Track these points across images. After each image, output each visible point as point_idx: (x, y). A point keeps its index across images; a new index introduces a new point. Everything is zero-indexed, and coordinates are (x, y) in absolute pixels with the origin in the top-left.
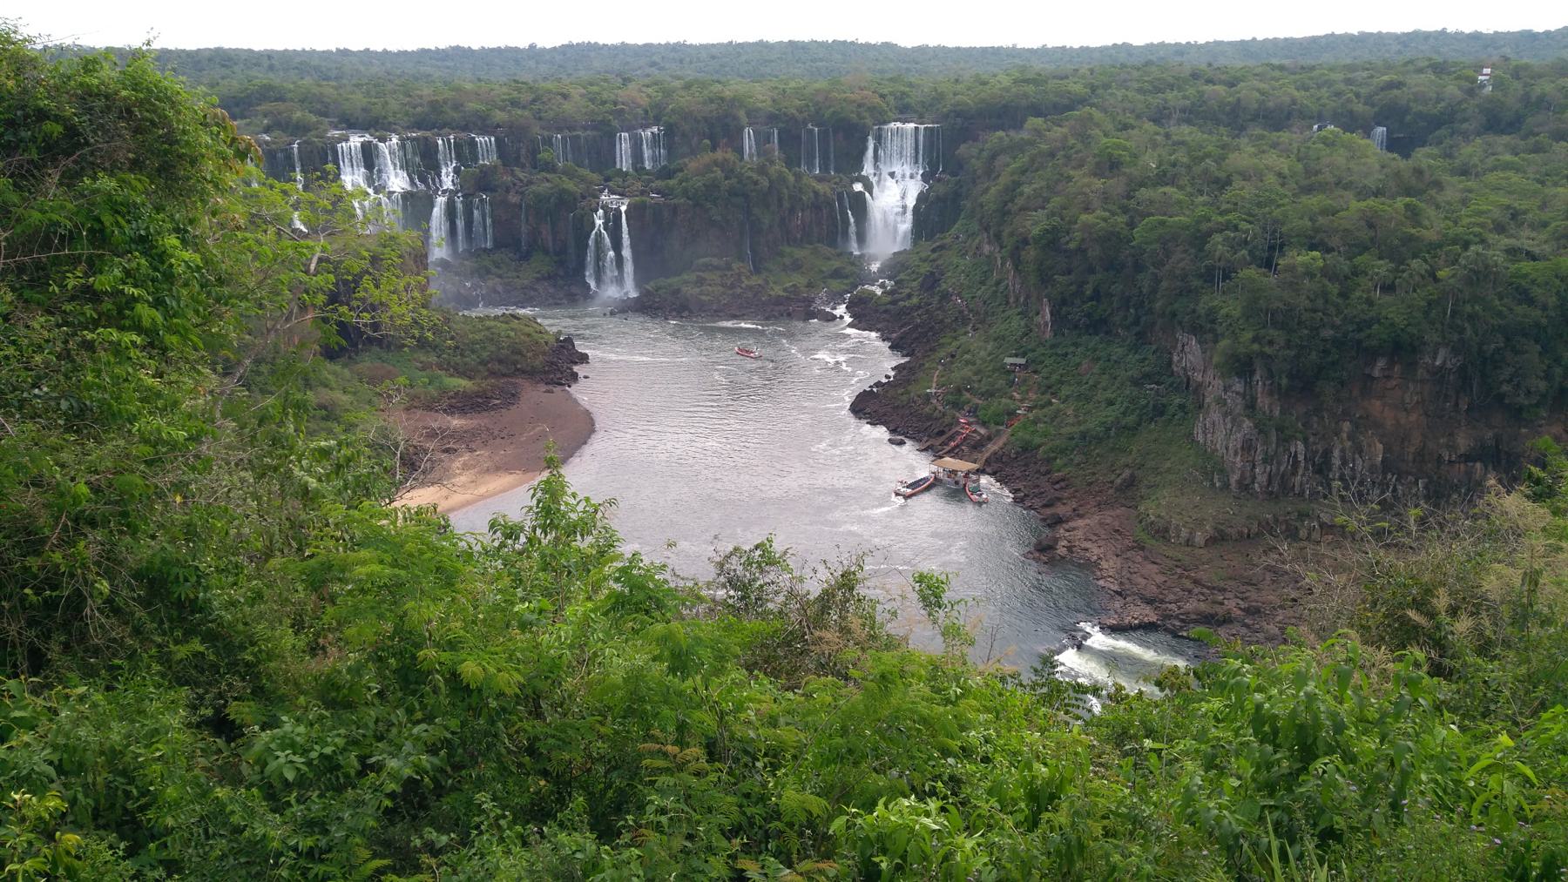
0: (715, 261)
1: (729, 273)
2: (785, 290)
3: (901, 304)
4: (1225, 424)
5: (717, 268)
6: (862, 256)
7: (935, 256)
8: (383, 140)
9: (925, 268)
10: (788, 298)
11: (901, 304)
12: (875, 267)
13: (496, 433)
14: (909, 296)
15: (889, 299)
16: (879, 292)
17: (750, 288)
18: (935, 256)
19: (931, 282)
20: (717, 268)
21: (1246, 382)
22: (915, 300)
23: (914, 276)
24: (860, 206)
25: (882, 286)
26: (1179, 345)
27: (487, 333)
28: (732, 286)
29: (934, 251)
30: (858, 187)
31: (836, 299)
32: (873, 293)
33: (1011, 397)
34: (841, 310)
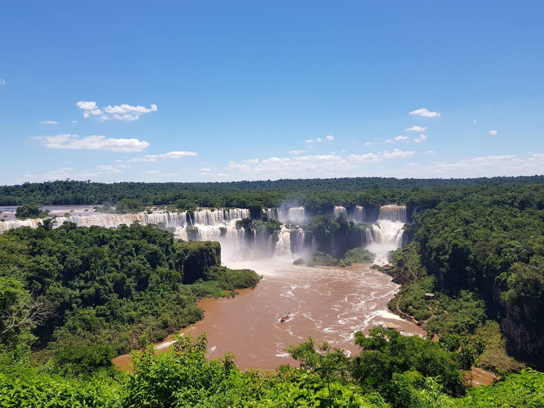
1: (325, 257)
4: (513, 325)
5: (320, 255)
7: (403, 253)
8: (212, 211)
9: (399, 258)
22: (395, 270)
23: (396, 261)
27: (237, 275)
29: (403, 251)
30: (375, 228)
33: (428, 309)
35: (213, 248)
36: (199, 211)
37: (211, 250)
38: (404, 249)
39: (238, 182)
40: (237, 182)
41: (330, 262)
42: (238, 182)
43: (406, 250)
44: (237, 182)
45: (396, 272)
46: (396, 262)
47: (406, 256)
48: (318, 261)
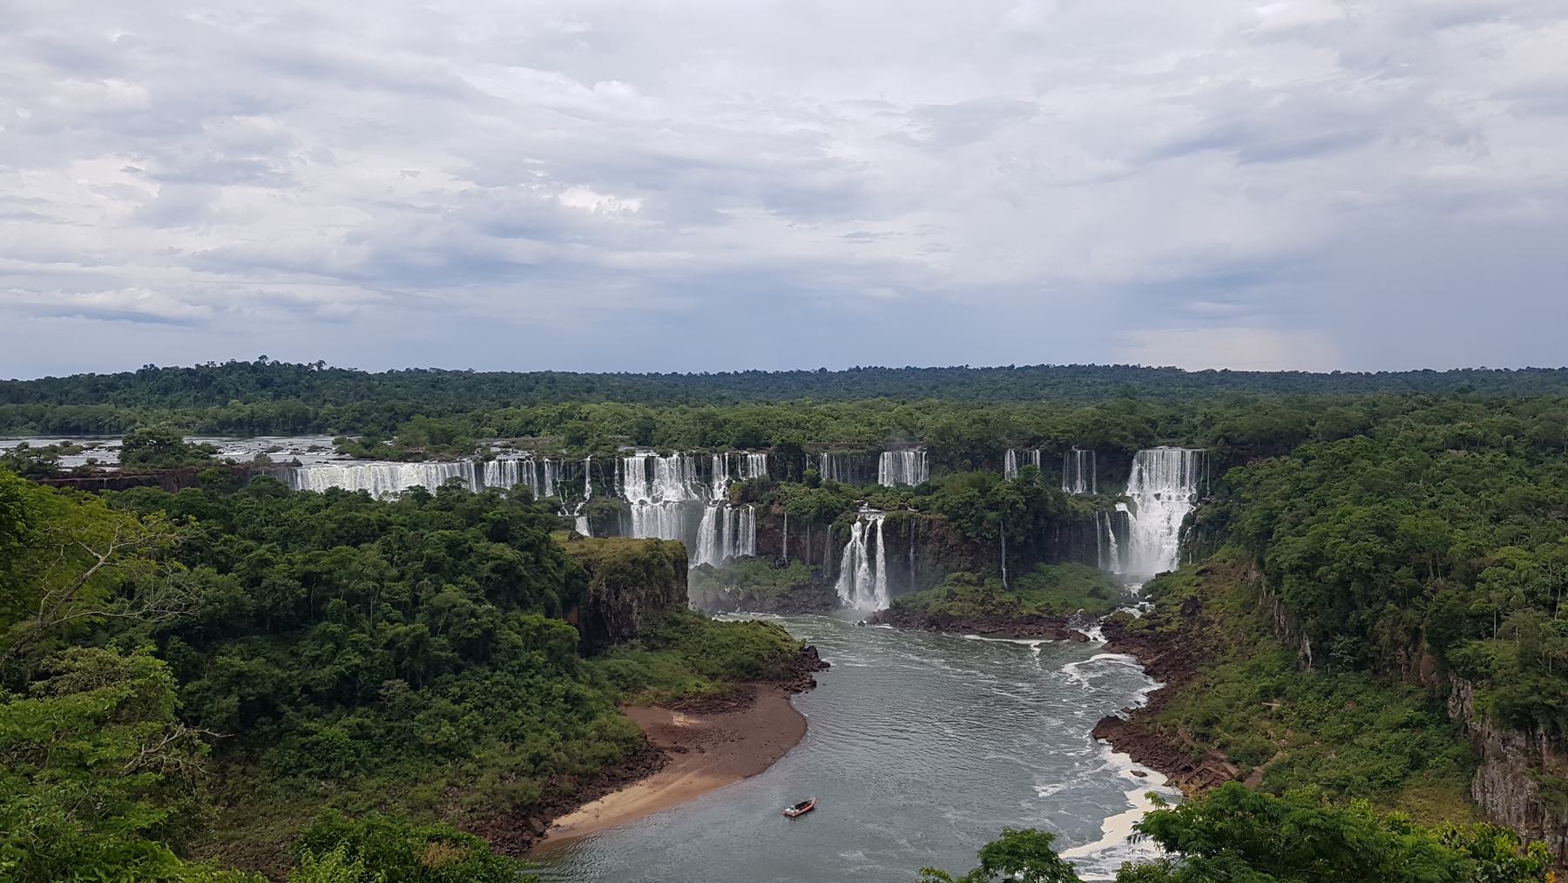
0: (967, 575)
2: (1037, 609)
3: (1158, 629)
5: (969, 582)
6: (1123, 576)
9: (1189, 592)
10: (1040, 617)
11: (1158, 629)
12: (1136, 588)
13: (726, 736)
14: (1168, 621)
15: (1146, 623)
16: (1138, 615)
17: (1002, 604)
18: (1201, 579)
19: (1192, 607)
20: (969, 582)
21: (1528, 735)
22: (1174, 626)
24: (1121, 526)
25: (1142, 609)
26: (1454, 691)
28: (983, 603)
29: (1198, 574)
30: (1121, 507)
31: (1089, 620)
32: (1132, 616)
34: (1095, 633)
35: (666, 560)
36: (627, 454)
37: (661, 564)
38: (1200, 569)
39: (735, 372)
40: (732, 373)
41: (994, 602)
42: (735, 372)
43: (1204, 571)
44: (732, 373)
45: (1177, 633)
46: (1177, 605)
47: (1203, 587)
48: (960, 601)
